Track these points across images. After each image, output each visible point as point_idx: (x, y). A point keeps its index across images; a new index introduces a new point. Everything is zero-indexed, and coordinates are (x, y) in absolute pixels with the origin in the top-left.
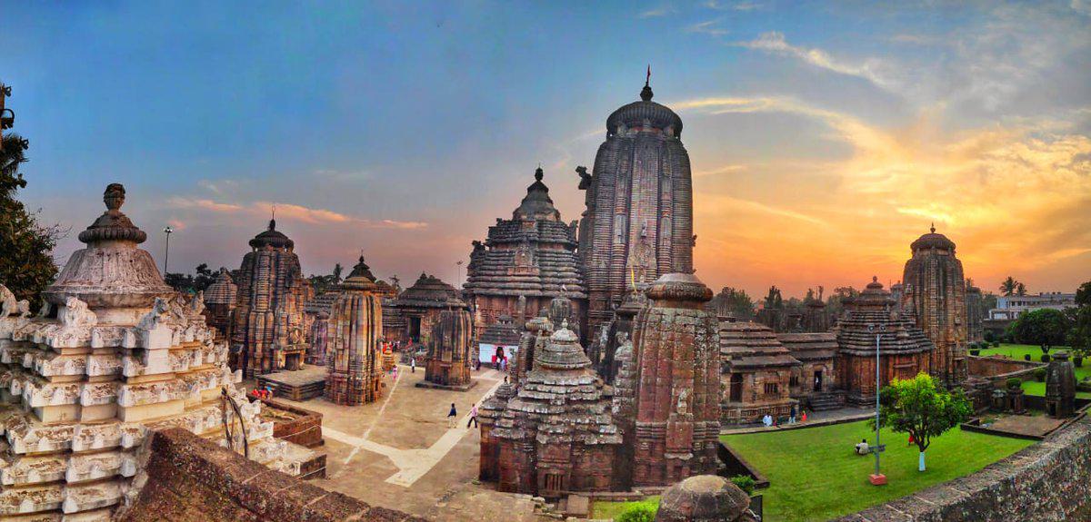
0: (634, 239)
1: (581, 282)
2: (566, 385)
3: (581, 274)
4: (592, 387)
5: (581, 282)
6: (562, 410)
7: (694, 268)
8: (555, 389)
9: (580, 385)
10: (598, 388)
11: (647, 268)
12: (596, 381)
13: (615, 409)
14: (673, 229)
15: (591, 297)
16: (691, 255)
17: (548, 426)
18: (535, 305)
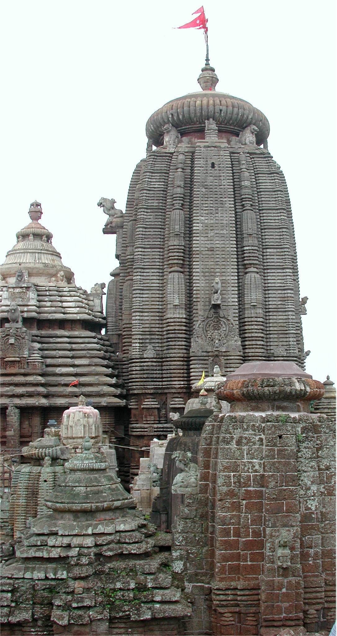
0: (201, 311)
1: (114, 381)
2: (93, 534)
3: (113, 368)
4: (137, 534)
5: (114, 381)
6: (91, 571)
7: (306, 350)
8: (76, 541)
9: (117, 532)
10: (148, 536)
11: (226, 354)
12: (144, 526)
13: (178, 566)
14: (266, 289)
15: (133, 405)
16: (299, 328)
17: (70, 597)
18: (37, 420)
